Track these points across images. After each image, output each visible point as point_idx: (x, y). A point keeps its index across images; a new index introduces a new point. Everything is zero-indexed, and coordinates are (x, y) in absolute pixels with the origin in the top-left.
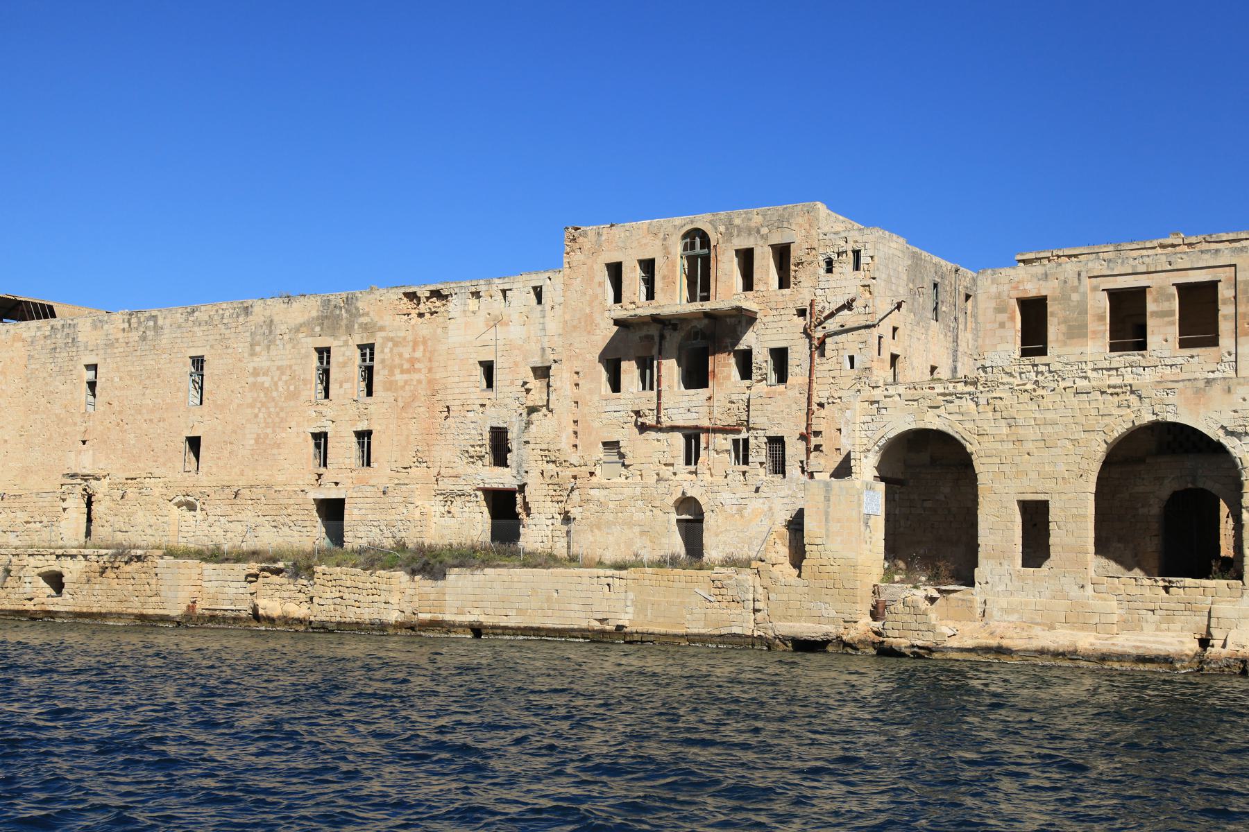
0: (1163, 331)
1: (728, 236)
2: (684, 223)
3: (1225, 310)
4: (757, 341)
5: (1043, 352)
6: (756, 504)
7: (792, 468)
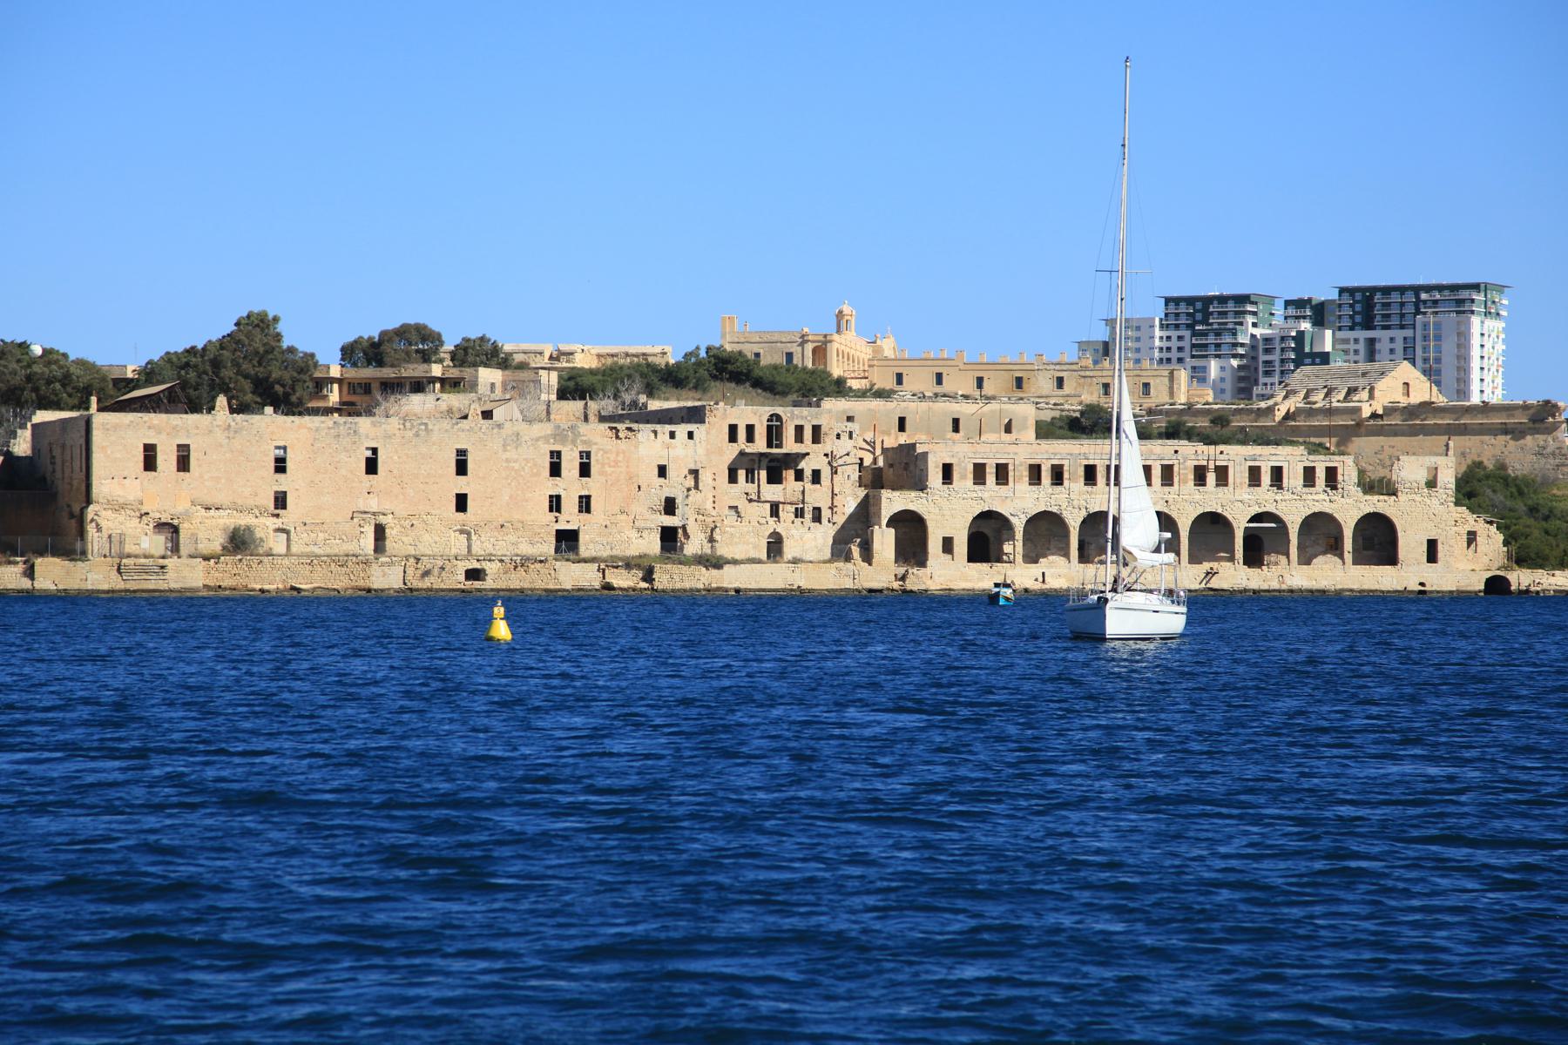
0: (991, 478)
1: (792, 418)
3: (1011, 474)
4: (807, 466)
6: (809, 535)
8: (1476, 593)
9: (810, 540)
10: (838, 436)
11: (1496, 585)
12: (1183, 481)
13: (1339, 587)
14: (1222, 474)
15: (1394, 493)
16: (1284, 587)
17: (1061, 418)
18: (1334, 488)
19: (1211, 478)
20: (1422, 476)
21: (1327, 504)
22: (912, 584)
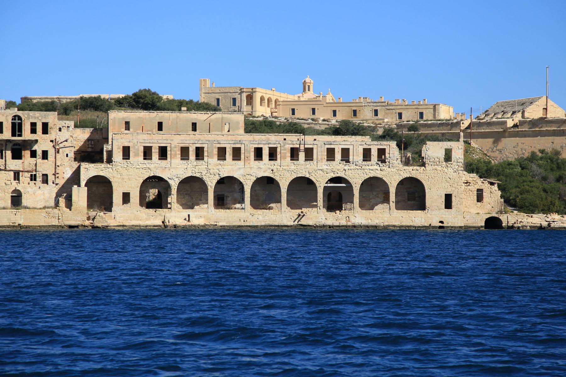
0: (155, 155)
1: (28, 118)
3: (169, 153)
5: (129, 159)
6: (39, 192)
7: (50, 182)
8: (479, 228)
9: (39, 196)
10: (60, 130)
11: (493, 223)
13: (386, 224)
14: (309, 154)
15: (423, 165)
16: (349, 224)
17: (330, 128)
18: (384, 161)
19: (302, 155)
20: (441, 154)
21: (379, 172)
22: (99, 223)
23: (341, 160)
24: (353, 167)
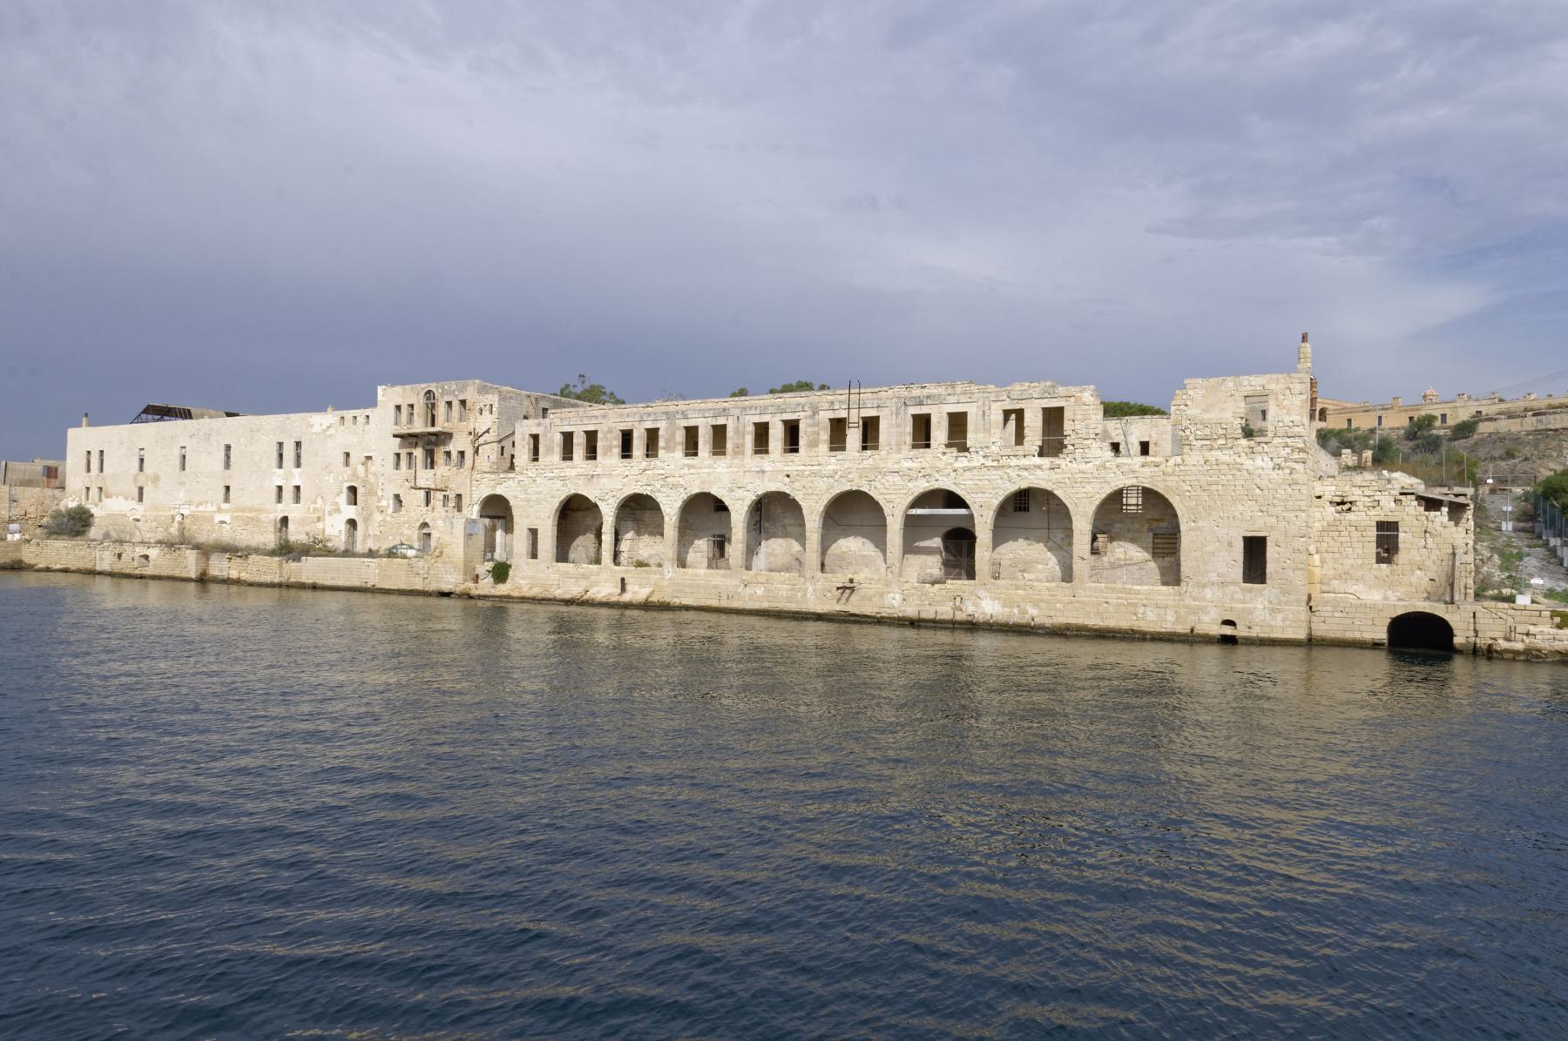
0: (579, 451)
2: (425, 387)
4: (453, 447)
12: (814, 444)
19: (854, 436)
20: (1231, 413)
23: (948, 446)
24: (976, 460)
